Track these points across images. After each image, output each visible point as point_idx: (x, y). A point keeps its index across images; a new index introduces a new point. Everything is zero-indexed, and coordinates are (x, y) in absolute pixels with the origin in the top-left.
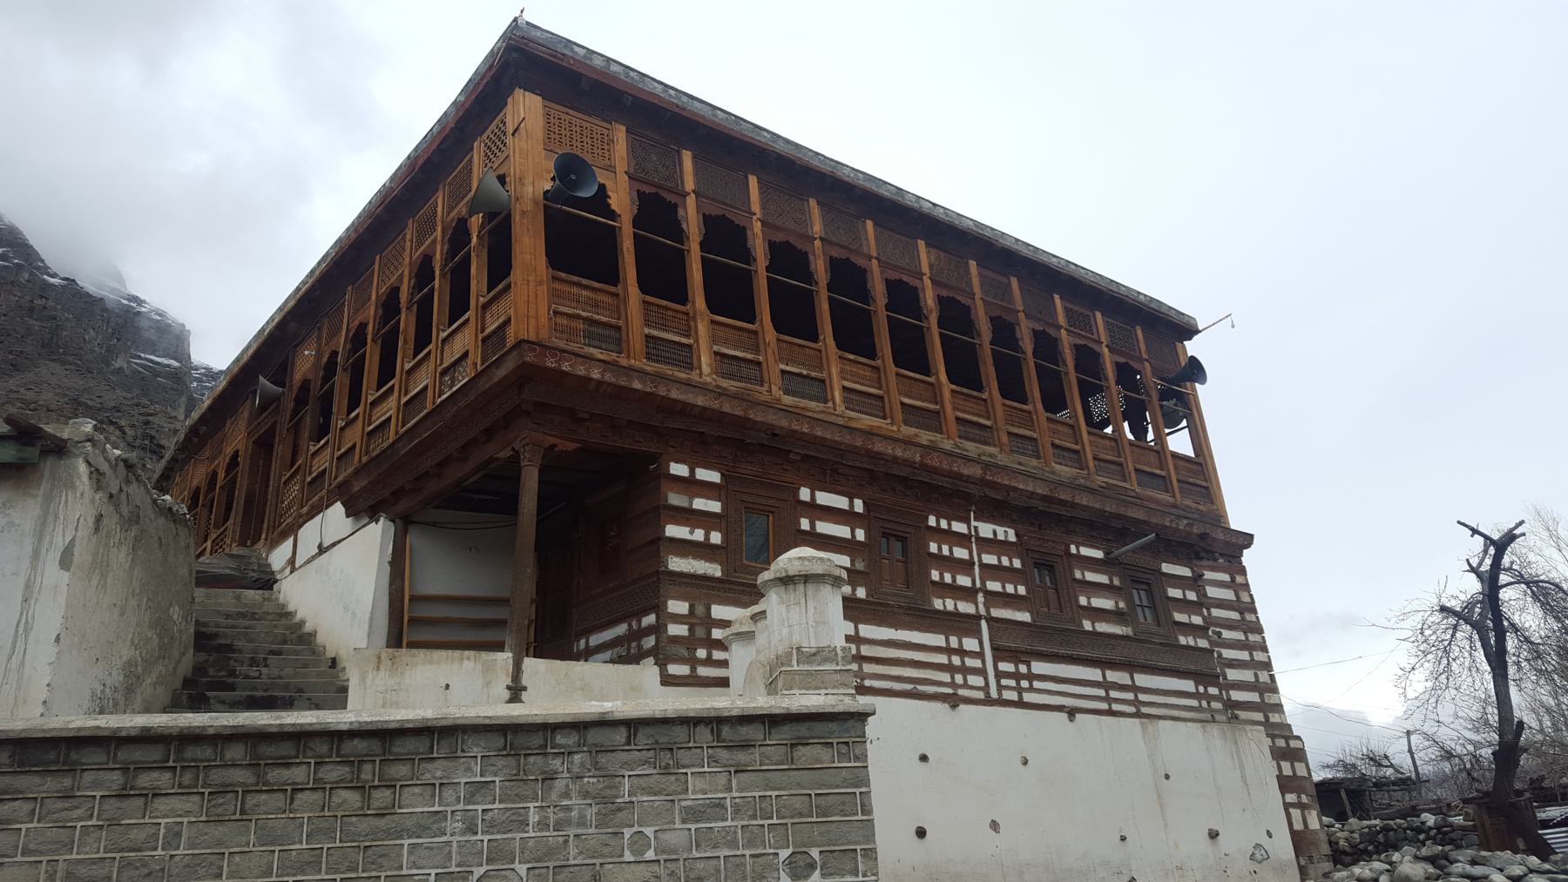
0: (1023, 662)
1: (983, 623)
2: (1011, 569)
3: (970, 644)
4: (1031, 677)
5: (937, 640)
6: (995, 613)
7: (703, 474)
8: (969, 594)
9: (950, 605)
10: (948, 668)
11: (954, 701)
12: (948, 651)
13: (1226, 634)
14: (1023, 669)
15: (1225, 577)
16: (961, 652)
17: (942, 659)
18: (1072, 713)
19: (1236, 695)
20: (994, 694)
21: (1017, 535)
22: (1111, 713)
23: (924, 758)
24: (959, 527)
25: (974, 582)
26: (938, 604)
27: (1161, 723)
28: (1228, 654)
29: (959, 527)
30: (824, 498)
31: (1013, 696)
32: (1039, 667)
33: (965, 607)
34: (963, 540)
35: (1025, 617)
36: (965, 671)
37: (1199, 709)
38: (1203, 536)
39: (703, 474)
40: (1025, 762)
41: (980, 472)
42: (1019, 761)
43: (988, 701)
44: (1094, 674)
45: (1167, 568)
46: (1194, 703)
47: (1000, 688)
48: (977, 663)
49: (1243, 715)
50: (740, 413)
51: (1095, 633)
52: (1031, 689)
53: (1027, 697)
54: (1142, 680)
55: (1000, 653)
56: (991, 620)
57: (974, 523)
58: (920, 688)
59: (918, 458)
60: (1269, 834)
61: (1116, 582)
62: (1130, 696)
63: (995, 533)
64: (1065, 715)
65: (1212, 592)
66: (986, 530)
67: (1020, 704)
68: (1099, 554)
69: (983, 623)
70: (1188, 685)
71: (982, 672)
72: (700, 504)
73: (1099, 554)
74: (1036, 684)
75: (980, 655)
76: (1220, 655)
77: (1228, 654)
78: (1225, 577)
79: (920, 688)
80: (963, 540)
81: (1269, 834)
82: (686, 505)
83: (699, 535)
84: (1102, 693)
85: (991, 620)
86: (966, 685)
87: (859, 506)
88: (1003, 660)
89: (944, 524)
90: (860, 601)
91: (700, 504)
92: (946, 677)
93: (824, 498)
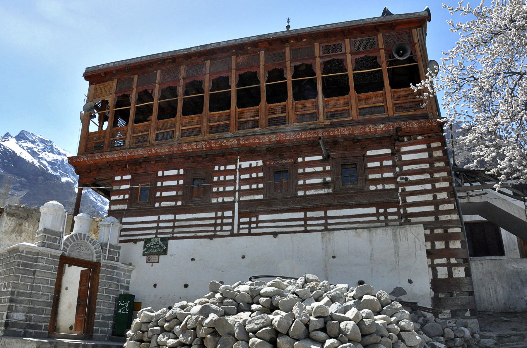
0: (254, 217)
1: (237, 205)
2: (258, 178)
3: (228, 214)
4: (257, 222)
5: (213, 215)
6: (242, 199)
7: (125, 177)
8: (231, 194)
9: (220, 200)
10: (215, 225)
11: (211, 237)
12: (216, 218)
13: (411, 178)
14: (254, 219)
15: (424, 146)
16: (223, 218)
17: (213, 222)
18: (275, 234)
19: (410, 210)
20: (235, 231)
21: (263, 162)
22: (306, 231)
23: (193, 259)
24: (229, 167)
25: (235, 188)
26: (214, 201)
27: (336, 232)
28: (409, 189)
29: (229, 167)
30: (167, 173)
31: (246, 231)
32: (261, 217)
33: (227, 199)
34: (232, 172)
35: (261, 197)
36: (222, 224)
37: (378, 221)
38: (398, 129)
39: (125, 177)
40: (243, 257)
41: (236, 142)
42: (241, 257)
43: (232, 235)
44: (301, 215)
45: (369, 153)
46: (375, 218)
47: (239, 229)
48: (230, 221)
49: (413, 220)
50: (129, 155)
51: (305, 196)
52: (257, 227)
53: (253, 231)
54: (330, 213)
55: (241, 216)
56: (239, 201)
57: (239, 164)
58: (198, 234)
59: (204, 146)
60: (410, 282)
61: (328, 168)
62: (323, 222)
63: (251, 165)
64: (272, 236)
65: (405, 158)
66: (245, 165)
67: (250, 234)
68: (320, 158)
69: (237, 205)
70: (373, 210)
71: (232, 224)
72: (123, 187)
73: (320, 158)
74: (260, 225)
75: (233, 217)
76: (403, 190)
77: (409, 189)
78: (424, 146)
79: (198, 234)
80: (232, 172)
81: (410, 282)
82: (118, 188)
83: (121, 197)
84: (302, 223)
85: (239, 201)
86: (222, 230)
87: (182, 172)
88: (242, 217)
89: (222, 168)
90: (179, 206)
91: (123, 187)
92: (212, 229)
93: (167, 173)
